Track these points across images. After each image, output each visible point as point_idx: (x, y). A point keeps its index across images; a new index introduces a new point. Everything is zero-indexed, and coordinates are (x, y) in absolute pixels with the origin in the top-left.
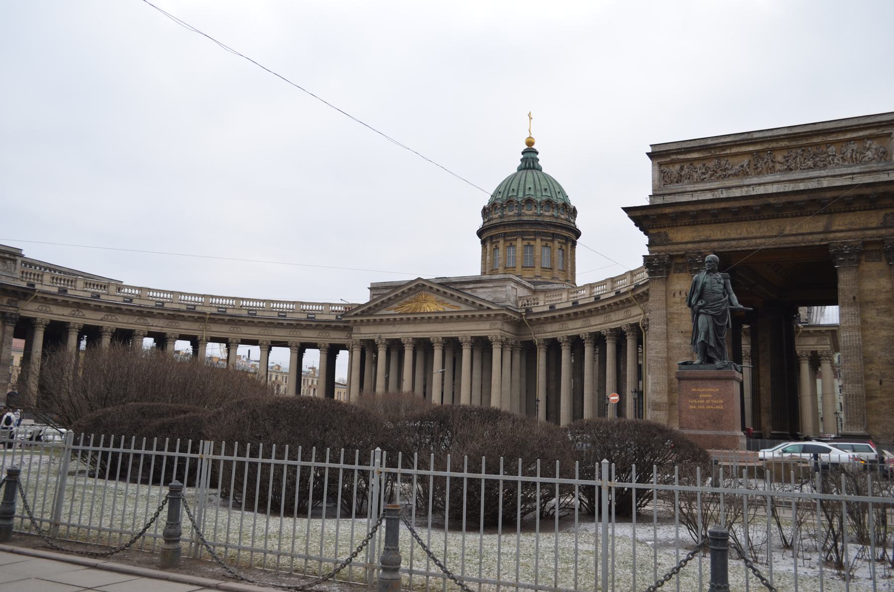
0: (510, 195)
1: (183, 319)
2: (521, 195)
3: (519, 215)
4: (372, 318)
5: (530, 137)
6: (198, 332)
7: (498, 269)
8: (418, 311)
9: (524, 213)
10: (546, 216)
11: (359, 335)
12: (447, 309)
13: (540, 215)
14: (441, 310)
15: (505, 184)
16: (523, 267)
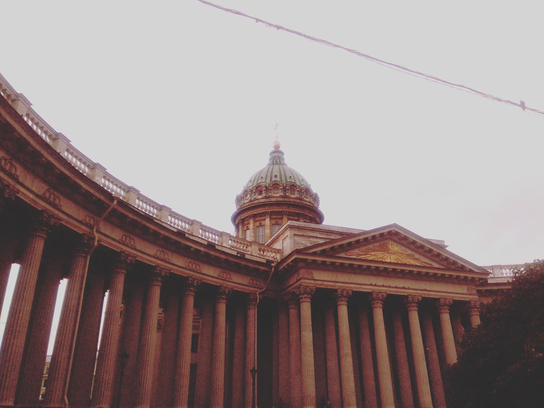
0: (288, 180)
2: (298, 183)
5: (276, 142)
9: (303, 198)
11: (312, 282)
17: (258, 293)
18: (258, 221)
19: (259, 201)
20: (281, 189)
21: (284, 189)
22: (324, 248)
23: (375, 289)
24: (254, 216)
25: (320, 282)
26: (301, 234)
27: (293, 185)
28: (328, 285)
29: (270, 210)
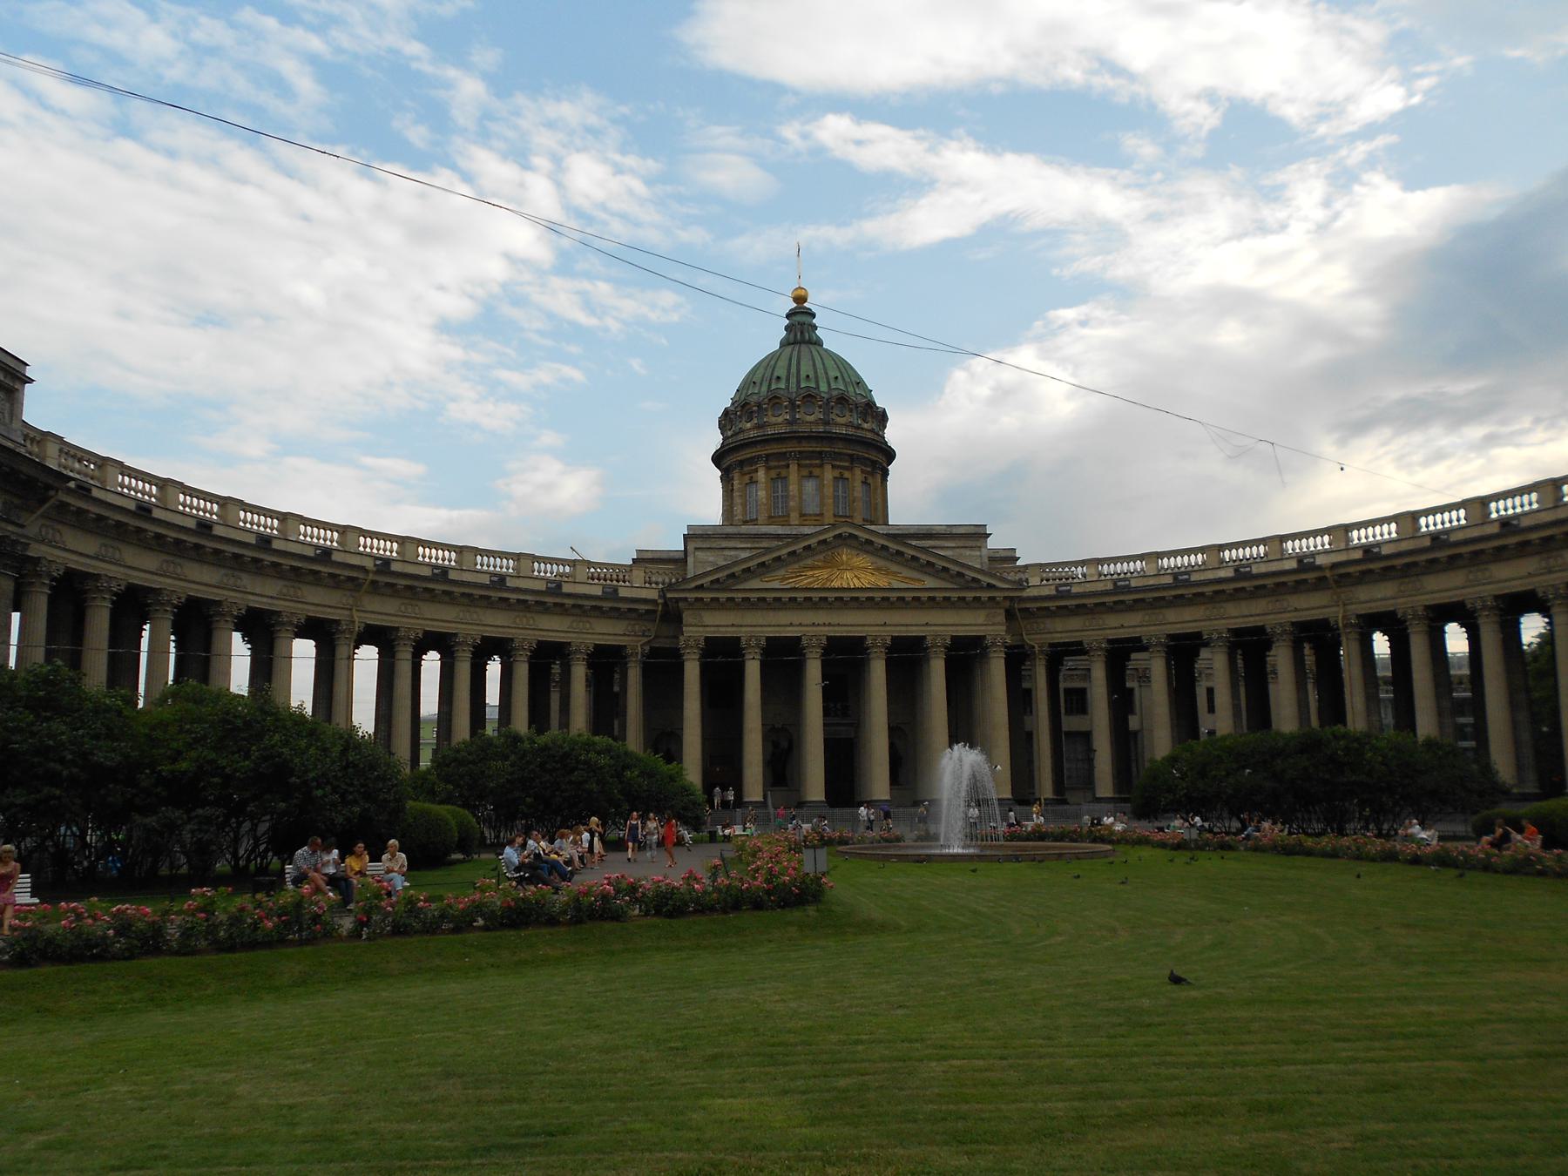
1: (316, 579)
2: (823, 388)
3: (826, 423)
4: (740, 595)
5: (800, 288)
6: (339, 611)
7: (757, 519)
8: (836, 584)
9: (833, 419)
10: (866, 430)
11: (701, 629)
12: (896, 585)
13: (858, 427)
14: (883, 582)
15: (783, 363)
16: (835, 516)
17: (641, 645)
18: (746, 474)
19: (746, 435)
20: (786, 407)
21: (793, 406)
22: (716, 577)
23: (808, 632)
24: (741, 463)
25: (712, 629)
26: (708, 546)
27: (810, 395)
28: (727, 632)
29: (765, 452)
